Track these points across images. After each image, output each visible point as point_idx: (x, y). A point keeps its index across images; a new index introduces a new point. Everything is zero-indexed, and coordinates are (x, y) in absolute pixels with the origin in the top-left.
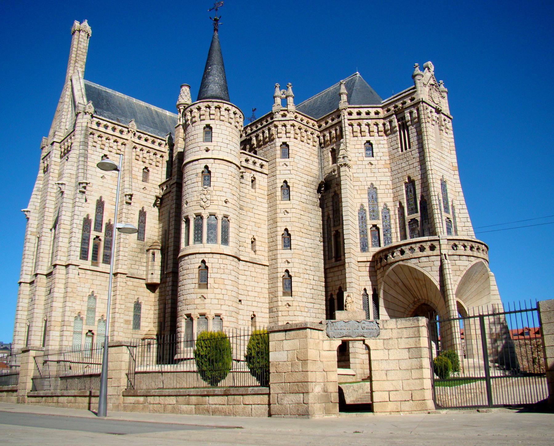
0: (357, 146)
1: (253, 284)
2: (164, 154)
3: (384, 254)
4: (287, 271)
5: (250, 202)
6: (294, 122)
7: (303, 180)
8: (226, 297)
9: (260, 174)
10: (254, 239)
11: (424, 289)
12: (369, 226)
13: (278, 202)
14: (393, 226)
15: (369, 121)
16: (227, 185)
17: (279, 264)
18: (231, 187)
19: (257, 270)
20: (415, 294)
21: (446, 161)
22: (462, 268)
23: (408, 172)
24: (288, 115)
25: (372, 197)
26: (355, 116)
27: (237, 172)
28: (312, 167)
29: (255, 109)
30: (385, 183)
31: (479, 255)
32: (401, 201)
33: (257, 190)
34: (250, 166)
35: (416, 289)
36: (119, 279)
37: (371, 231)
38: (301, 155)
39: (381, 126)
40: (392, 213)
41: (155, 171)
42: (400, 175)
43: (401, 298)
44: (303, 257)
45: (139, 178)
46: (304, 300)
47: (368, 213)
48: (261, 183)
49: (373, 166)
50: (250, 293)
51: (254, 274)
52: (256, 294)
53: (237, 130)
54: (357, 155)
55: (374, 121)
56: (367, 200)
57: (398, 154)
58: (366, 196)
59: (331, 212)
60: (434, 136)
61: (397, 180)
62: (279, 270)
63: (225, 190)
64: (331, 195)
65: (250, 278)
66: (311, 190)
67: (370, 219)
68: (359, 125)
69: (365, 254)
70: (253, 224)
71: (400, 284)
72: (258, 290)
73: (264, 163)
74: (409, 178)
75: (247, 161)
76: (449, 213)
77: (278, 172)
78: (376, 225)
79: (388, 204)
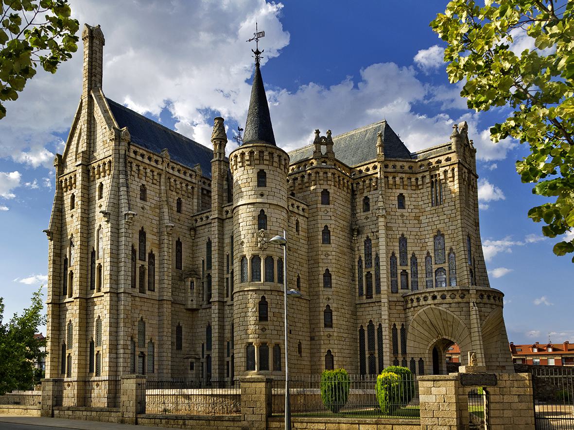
0: (391, 198)
1: (299, 316)
2: (194, 185)
3: (416, 297)
4: (328, 306)
6: (334, 170)
7: (340, 225)
9: (301, 218)
11: (450, 329)
12: (399, 271)
13: (320, 245)
14: (419, 272)
15: (404, 175)
17: (321, 300)
20: (440, 331)
23: (438, 226)
24: (328, 163)
25: (403, 245)
26: (390, 169)
28: (347, 213)
30: (415, 234)
32: (430, 251)
33: (301, 233)
34: (296, 210)
35: (441, 328)
36: (165, 306)
37: (401, 275)
38: (339, 202)
39: (413, 180)
40: (418, 261)
41: (187, 202)
42: (429, 228)
43: (427, 334)
44: (340, 294)
45: (174, 208)
46: (342, 331)
47: (398, 260)
48: (303, 226)
49: (405, 218)
54: (391, 206)
55: (408, 175)
56: (398, 248)
57: (428, 209)
58: (397, 244)
59: (363, 256)
61: (426, 232)
62: (322, 305)
64: (363, 240)
65: (296, 311)
66: (346, 235)
67: (400, 265)
68: (394, 178)
69: (395, 295)
70: (298, 263)
71: (428, 323)
72: (303, 321)
73: (305, 207)
74: (439, 231)
75: (293, 205)
77: (319, 217)
78: (406, 270)
79: (416, 253)
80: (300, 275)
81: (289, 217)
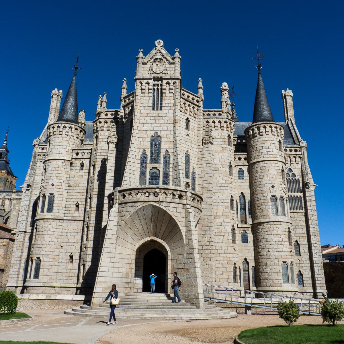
1: (73, 234)
5: (77, 180)
8: (44, 246)
10: (78, 204)
16: (54, 175)
18: (57, 175)
19: (72, 224)
21: (164, 118)
22: (126, 214)
27: (64, 164)
29: (233, 87)
31: (146, 199)
50: (70, 241)
51: (74, 228)
52: (75, 241)
53: (68, 137)
60: (151, 102)
63: (52, 178)
65: (72, 231)
76: (160, 163)
80: (80, 203)
81: (71, 164)
